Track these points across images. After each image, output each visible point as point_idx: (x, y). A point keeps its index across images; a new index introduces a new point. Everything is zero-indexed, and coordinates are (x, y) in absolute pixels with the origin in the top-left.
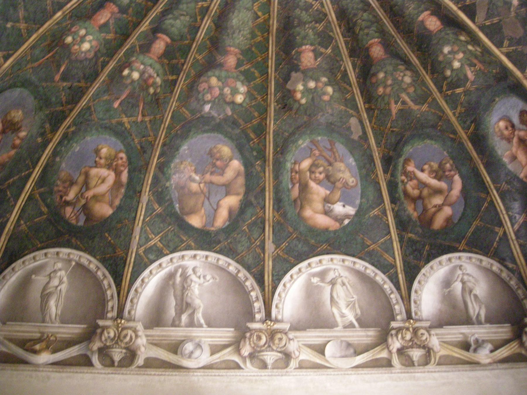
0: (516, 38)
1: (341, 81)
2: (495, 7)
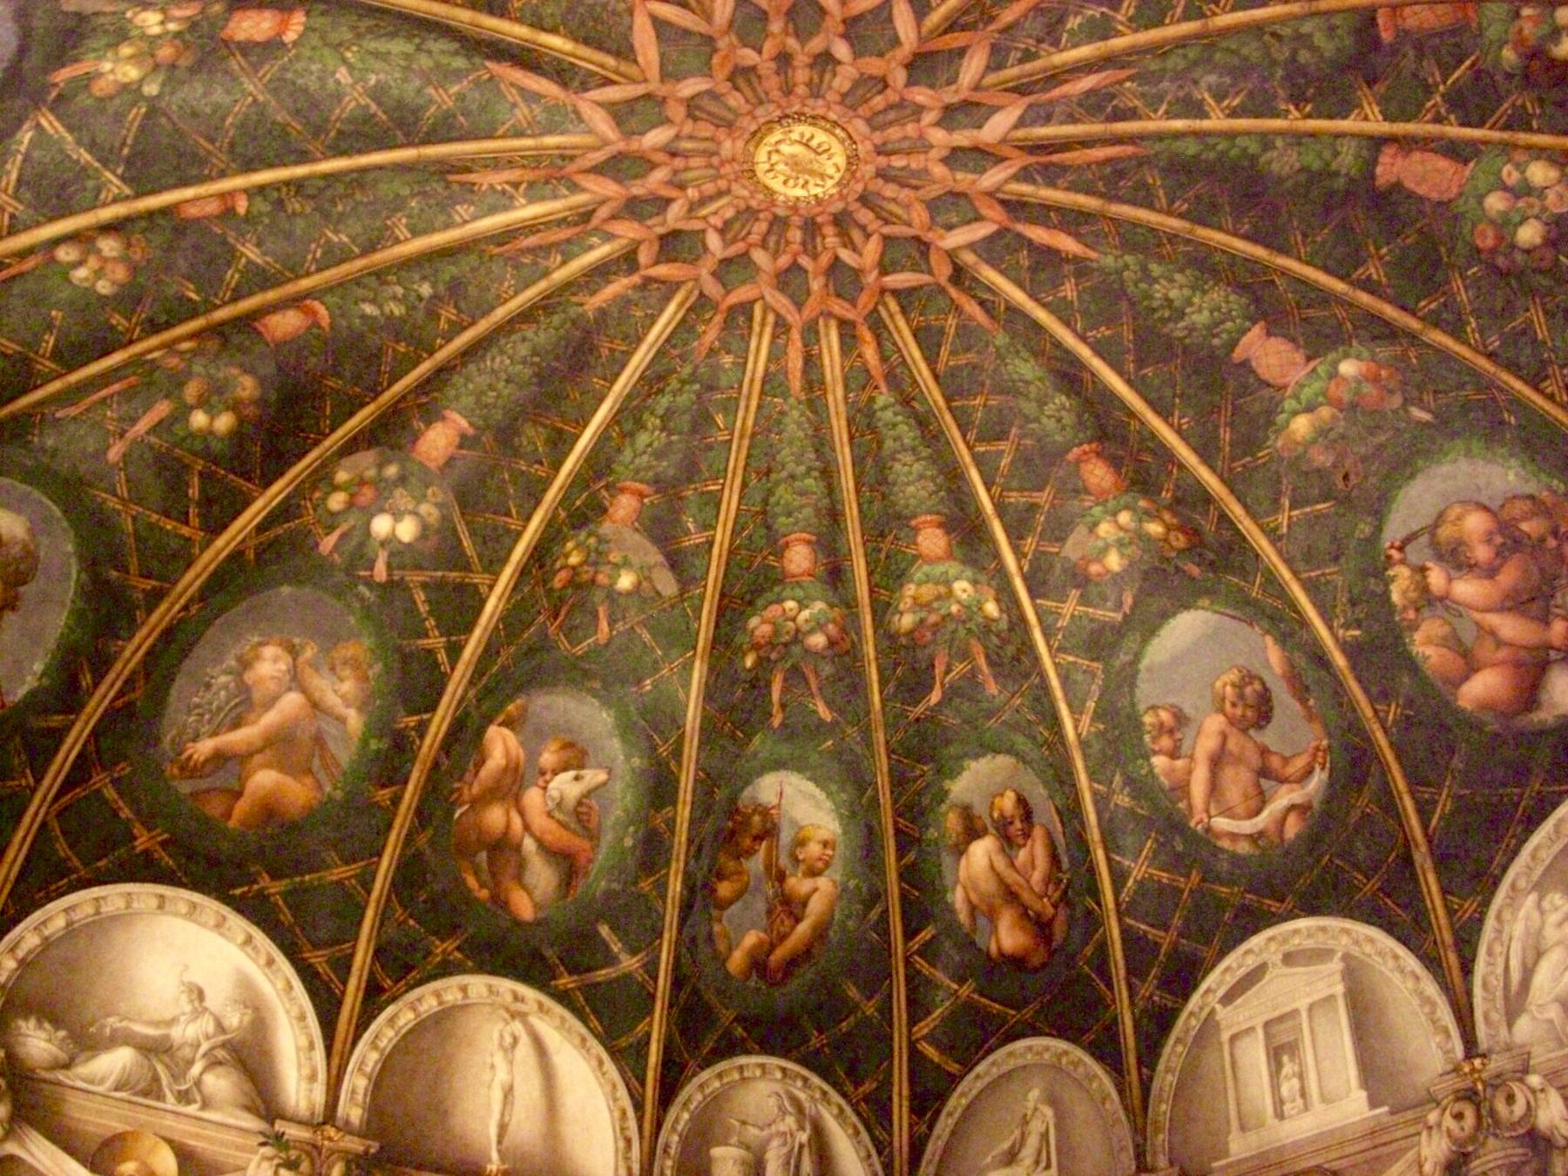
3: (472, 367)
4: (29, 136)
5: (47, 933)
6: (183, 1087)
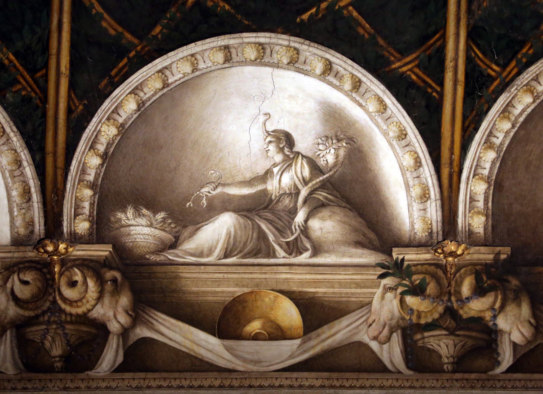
5: (121, 120)
6: (292, 238)
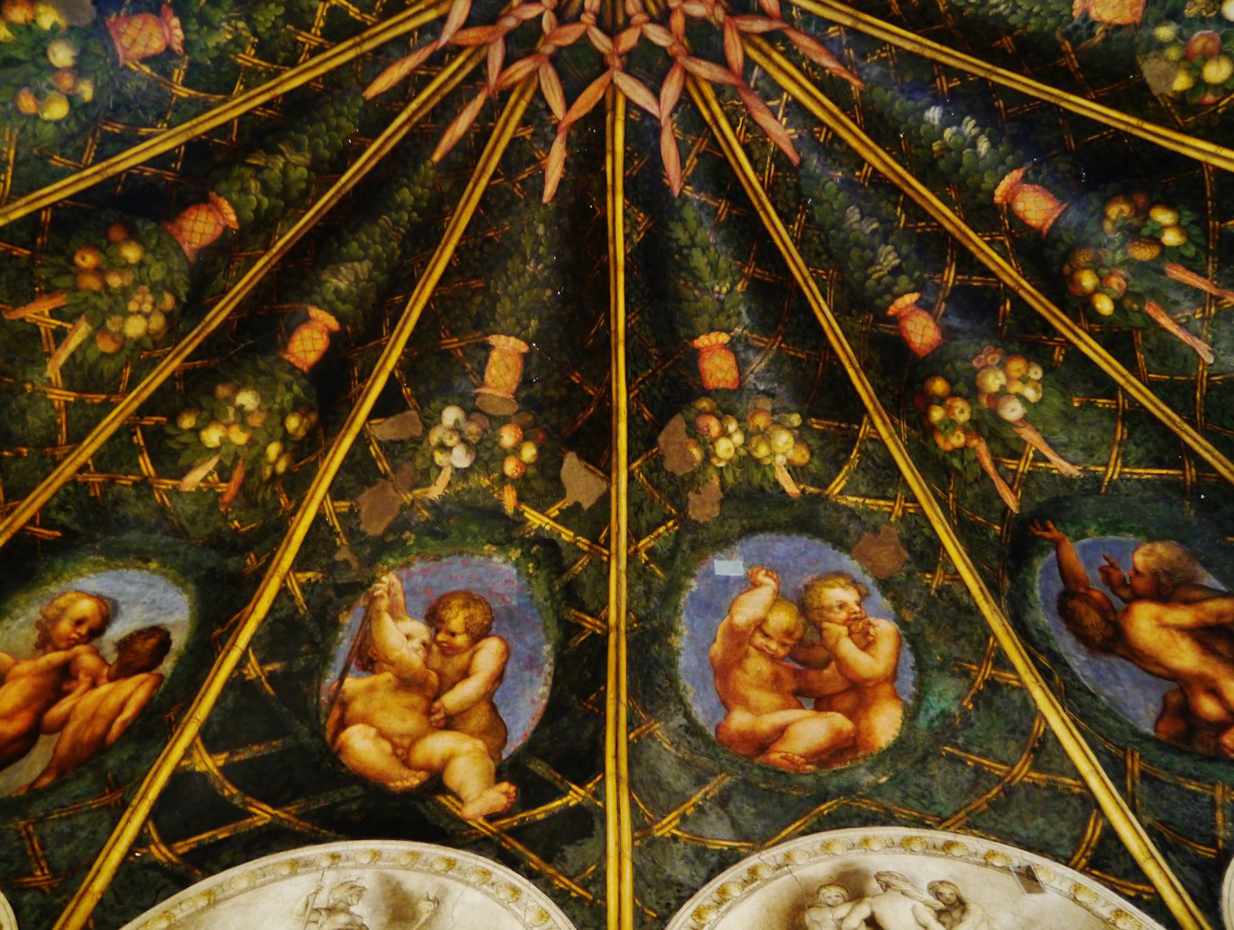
0: (359, 524)
1: (98, 134)
2: (410, 453)
3: (1013, 20)
4: (851, 499)
